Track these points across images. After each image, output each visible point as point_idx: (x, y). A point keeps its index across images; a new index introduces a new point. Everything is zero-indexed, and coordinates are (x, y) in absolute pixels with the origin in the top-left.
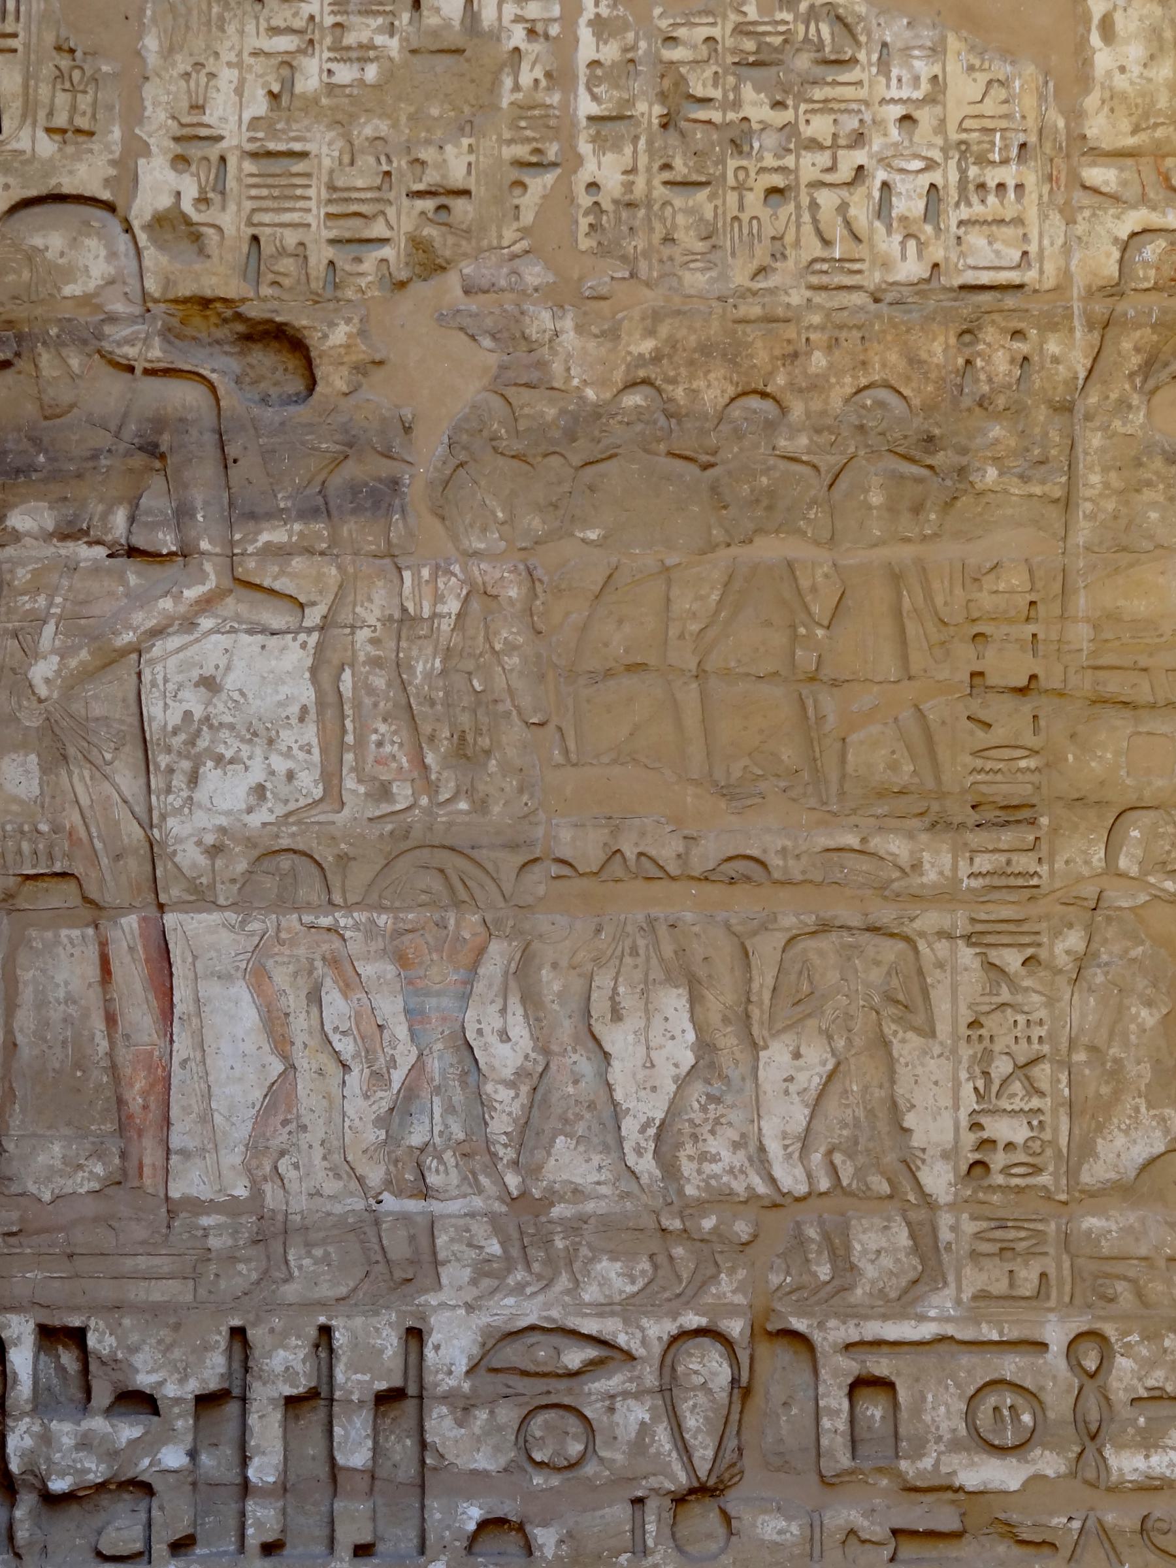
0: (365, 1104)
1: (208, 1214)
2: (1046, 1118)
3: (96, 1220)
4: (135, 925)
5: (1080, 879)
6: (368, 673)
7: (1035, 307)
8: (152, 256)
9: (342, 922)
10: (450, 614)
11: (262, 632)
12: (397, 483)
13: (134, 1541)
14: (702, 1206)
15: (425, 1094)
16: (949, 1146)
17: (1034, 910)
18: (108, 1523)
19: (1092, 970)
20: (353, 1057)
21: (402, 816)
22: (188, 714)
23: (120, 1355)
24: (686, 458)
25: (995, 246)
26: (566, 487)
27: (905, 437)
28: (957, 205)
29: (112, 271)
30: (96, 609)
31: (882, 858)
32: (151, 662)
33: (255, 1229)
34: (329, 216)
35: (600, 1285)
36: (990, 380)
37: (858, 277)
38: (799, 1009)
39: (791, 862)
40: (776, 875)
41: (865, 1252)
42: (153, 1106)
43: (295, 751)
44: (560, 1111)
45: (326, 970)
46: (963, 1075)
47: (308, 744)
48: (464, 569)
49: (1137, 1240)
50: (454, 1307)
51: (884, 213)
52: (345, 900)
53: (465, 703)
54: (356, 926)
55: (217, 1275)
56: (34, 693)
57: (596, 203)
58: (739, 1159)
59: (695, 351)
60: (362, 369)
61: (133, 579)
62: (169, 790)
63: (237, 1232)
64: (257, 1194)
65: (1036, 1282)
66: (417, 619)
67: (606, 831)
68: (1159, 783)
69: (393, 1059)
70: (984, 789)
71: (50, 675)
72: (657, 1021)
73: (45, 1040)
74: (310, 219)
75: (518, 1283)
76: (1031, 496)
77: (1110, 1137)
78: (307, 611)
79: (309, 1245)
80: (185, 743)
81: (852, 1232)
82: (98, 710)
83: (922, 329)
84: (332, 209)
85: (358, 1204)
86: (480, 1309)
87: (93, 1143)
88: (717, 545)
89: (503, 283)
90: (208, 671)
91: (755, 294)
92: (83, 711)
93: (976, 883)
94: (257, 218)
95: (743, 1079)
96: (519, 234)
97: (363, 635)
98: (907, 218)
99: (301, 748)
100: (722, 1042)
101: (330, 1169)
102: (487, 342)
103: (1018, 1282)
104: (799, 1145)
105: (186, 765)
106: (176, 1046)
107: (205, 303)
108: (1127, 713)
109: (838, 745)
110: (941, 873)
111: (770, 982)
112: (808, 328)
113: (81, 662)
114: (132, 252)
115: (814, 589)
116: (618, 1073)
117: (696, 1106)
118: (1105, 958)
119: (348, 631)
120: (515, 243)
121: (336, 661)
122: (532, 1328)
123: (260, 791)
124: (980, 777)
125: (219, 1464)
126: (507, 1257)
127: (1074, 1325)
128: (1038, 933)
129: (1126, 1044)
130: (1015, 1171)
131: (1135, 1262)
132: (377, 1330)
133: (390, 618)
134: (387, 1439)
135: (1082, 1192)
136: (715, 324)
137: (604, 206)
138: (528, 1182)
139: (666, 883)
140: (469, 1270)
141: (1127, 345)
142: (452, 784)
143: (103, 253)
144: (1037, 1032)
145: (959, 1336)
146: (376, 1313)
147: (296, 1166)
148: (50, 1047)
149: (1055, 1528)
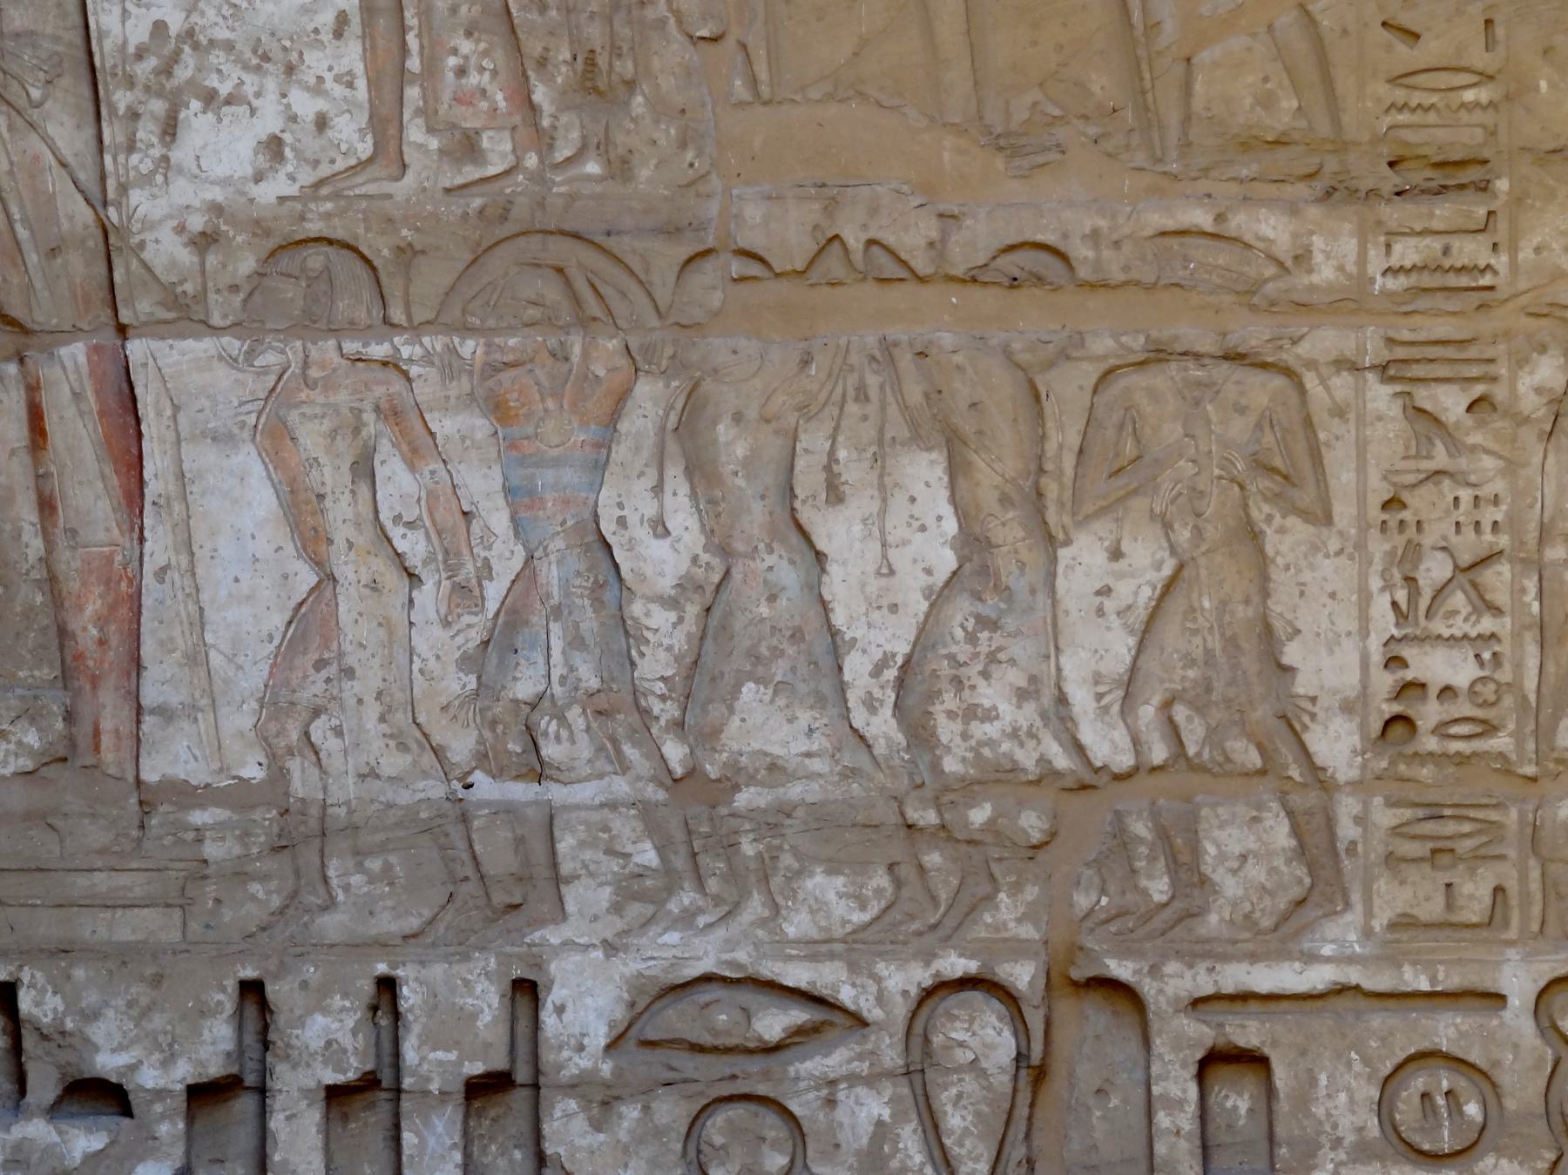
2: (1504, 648)
3: (29, 816)
4: (82, 359)
9: (406, 352)
14: (970, 789)
15: (537, 620)
16: (1352, 694)
17: (1487, 325)
20: (425, 563)
21: (497, 186)
22: (159, 27)
23: (69, 1025)
31: (1248, 246)
33: (276, 830)
35: (812, 912)
38: (1119, 482)
39: (1107, 253)
40: (1083, 273)
41: (1222, 857)
42: (114, 640)
43: (329, 84)
44: (747, 643)
45: (380, 426)
46: (1375, 583)
47: (349, 73)
50: (586, 947)
54: (427, 359)
55: (218, 901)
58: (1027, 715)
62: (131, 147)
63: (247, 834)
64: (278, 775)
65: (1488, 900)
67: (816, 206)
70: (1409, 136)
72: (898, 502)
75: (685, 910)
79: (359, 854)
80: (157, 72)
81: (1203, 826)
86: (626, 948)
87: (22, 698)
93: (1395, 284)
95: (1033, 592)
99: (337, 79)
100: (998, 534)
101: (391, 736)
103: (1461, 902)
104: (1120, 693)
105: (158, 106)
106: (148, 546)
109: (1180, 68)
111: (1074, 440)
116: (839, 585)
117: (959, 633)
122: (707, 979)
123: (274, 147)
124: (1402, 118)
126: (667, 870)
127: (1545, 967)
128: (1491, 361)
130: (1454, 730)
132: (466, 983)
134: (484, 1149)
135: (1559, 761)
138: (699, 753)
139: (911, 287)
140: (608, 890)
142: (575, 135)
144: (1490, 515)
145: (1368, 985)
146: (466, 958)
147: (338, 732)
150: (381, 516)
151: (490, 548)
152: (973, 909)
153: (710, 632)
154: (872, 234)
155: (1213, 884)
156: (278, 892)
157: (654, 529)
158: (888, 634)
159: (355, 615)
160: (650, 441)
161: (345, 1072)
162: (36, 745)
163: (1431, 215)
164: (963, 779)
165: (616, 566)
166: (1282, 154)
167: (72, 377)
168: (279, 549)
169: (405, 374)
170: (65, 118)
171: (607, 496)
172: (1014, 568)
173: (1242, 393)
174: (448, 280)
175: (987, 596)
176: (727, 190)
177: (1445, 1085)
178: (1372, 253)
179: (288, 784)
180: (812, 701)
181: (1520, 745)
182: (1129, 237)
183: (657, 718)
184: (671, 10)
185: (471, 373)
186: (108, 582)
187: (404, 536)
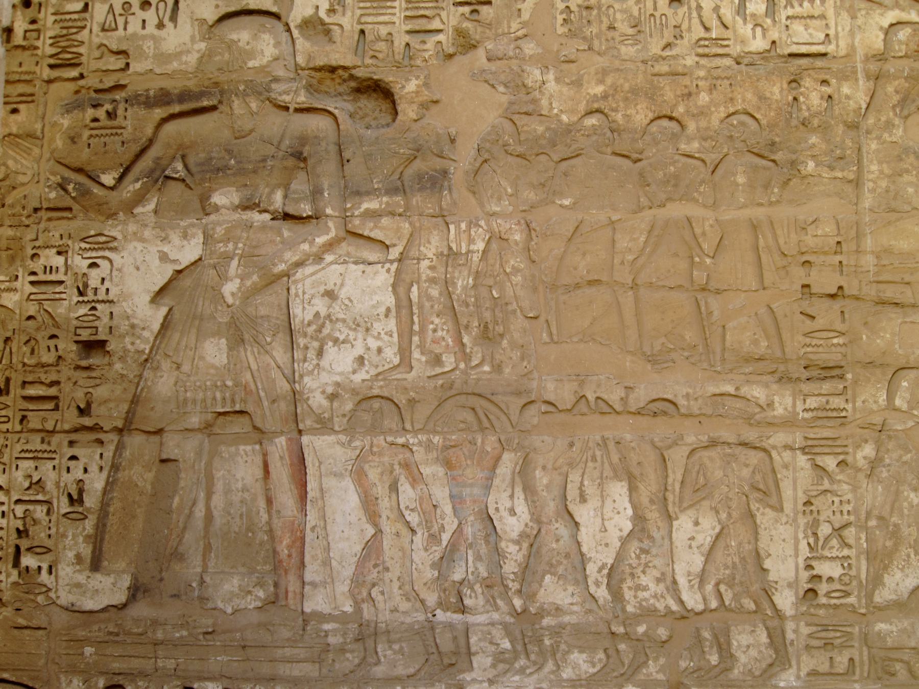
1: (328, 622)
2: (853, 562)
3: (260, 625)
4: (284, 443)
5: (872, 412)
6: (428, 287)
7: (835, 66)
8: (301, 43)
9: (411, 441)
10: (478, 251)
11: (363, 263)
12: (446, 173)
14: (638, 618)
15: (463, 549)
16: (792, 580)
17: (843, 432)
20: (418, 525)
21: (448, 375)
24: (624, 156)
25: (809, 31)
26: (550, 174)
27: (758, 143)
28: (786, 7)
29: (277, 52)
30: (262, 251)
31: (748, 400)
32: (296, 282)
33: (357, 632)
34: (406, 17)
35: (573, 668)
36: (809, 109)
37: (727, 49)
38: (699, 494)
40: (683, 410)
41: (739, 646)
42: (294, 555)
43: (383, 335)
44: (547, 559)
45: (401, 470)
46: (801, 535)
48: (487, 224)
49: (909, 637)
50: (481, 682)
51: (741, 11)
52: (413, 427)
53: (487, 305)
54: (420, 443)
55: (333, 661)
56: (225, 302)
57: (567, 7)
58: (661, 588)
59: (628, 92)
60: (425, 106)
61: (286, 234)
62: (305, 360)
65: (847, 664)
66: (458, 254)
69: (443, 526)
70: (811, 356)
71: (235, 290)
72: (609, 504)
73: (229, 514)
74: (395, 19)
75: (521, 667)
76: (835, 178)
77: (892, 573)
78: (390, 250)
79: (389, 641)
80: (316, 331)
81: (731, 634)
82: (263, 311)
83: (766, 79)
84: (408, 13)
85: (421, 617)
86: (497, 682)
87: (258, 578)
88: (643, 208)
89: (511, 54)
90: (330, 287)
91: (664, 59)
93: (807, 415)
94: (363, 20)
96: (521, 26)
97: (425, 264)
98: (755, 15)
99: (386, 334)
100: (649, 515)
102: (501, 89)
103: (836, 664)
104: (698, 580)
105: (316, 344)
106: (308, 518)
107: (333, 70)
108: (898, 310)
109: (720, 329)
110: (786, 409)
111: (679, 477)
112: (697, 79)
113: (253, 283)
114: (290, 42)
115: (704, 234)
116: (584, 535)
117: (633, 555)
118: (887, 461)
119: (415, 261)
120: (518, 30)
121: (408, 280)
123: (361, 360)
124: (809, 349)
126: (514, 650)
129: (902, 515)
130: (833, 595)
133: (442, 254)
135: (874, 607)
136: (640, 77)
137: (572, 9)
138: (528, 603)
139: (613, 416)
141: (890, 89)
142: (480, 355)
143: (272, 42)
144: (846, 508)
147: (382, 593)
148: (233, 518)
151: (444, 519)
152: (638, 667)
153: (532, 554)
155: (736, 657)
163: (821, 388)
164: (634, 614)
165: (495, 528)
166: (761, 364)
169: (411, 450)
170: (280, 349)
174: (429, 412)
176: (540, 378)
178: (798, 403)
179: (362, 614)
181: (859, 601)
186: (292, 531)
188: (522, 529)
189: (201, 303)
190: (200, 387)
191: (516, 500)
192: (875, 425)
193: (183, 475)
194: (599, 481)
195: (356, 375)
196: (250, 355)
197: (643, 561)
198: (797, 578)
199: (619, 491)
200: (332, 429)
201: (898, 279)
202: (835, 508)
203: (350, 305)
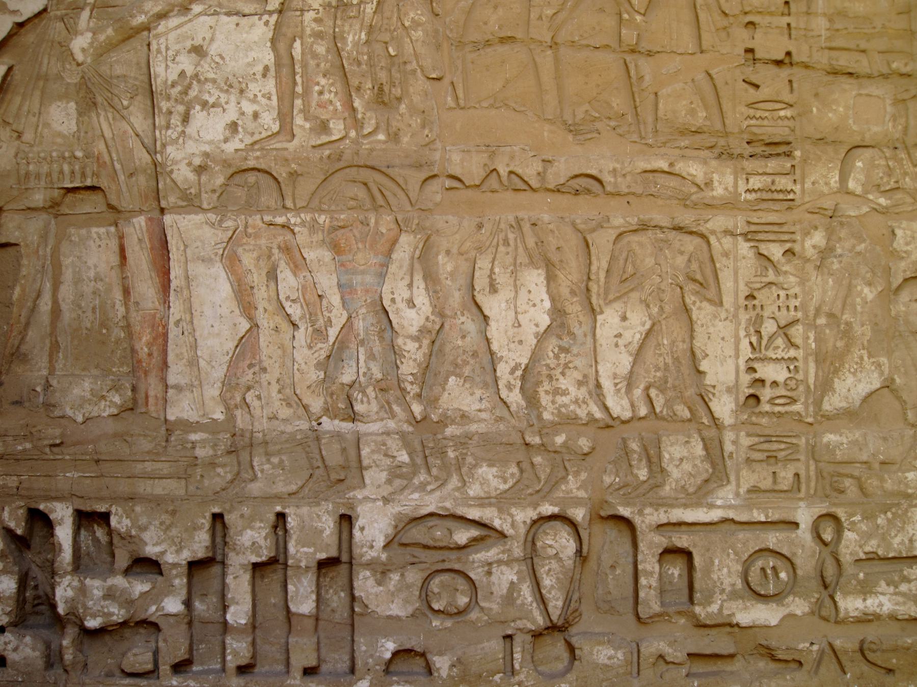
0: (309, 353)
1: (195, 432)
2: (800, 364)
3: (116, 435)
4: (143, 224)
5: (822, 195)
6: (313, 43)
9: (293, 221)
13: (147, 663)
15: (353, 346)
16: (731, 384)
18: (129, 649)
19: (830, 260)
20: (300, 319)
21: (337, 145)
22: (182, 74)
23: (133, 533)
31: (684, 178)
32: (157, 36)
33: (229, 443)
35: (481, 484)
38: (627, 284)
39: (619, 180)
40: (609, 188)
41: (672, 459)
42: (155, 354)
43: (259, 98)
44: (451, 358)
45: (281, 255)
46: (742, 333)
47: (269, 93)
49: (861, 449)
50: (375, 500)
52: (295, 205)
53: (383, 64)
54: (303, 224)
55: (202, 476)
56: (74, 59)
58: (582, 393)
62: (168, 127)
63: (216, 445)
64: (231, 417)
65: (791, 479)
68: (875, 129)
69: (330, 320)
70: (755, 130)
71: (85, 46)
72: (523, 295)
73: (80, 307)
75: (421, 483)
77: (843, 377)
79: (268, 454)
80: (181, 93)
81: (663, 445)
82: (119, 70)
85: (304, 425)
86: (393, 500)
90: (198, 42)
92: (108, 72)
93: (751, 197)
95: (585, 335)
97: (309, 16)
99: (263, 96)
100: (570, 309)
101: (284, 400)
103: (779, 480)
104: (625, 383)
105: (181, 108)
106: (172, 310)
109: (652, 97)
110: (726, 189)
111: (605, 265)
113: (108, 37)
116: (494, 331)
117: (551, 354)
118: (839, 251)
119: (298, 13)
121: (290, 35)
122: (431, 515)
123: (233, 127)
124: (753, 122)
125: (208, 609)
126: (413, 463)
127: (817, 510)
128: (793, 233)
129: (854, 312)
130: (777, 401)
131: (858, 465)
132: (318, 516)
134: (327, 591)
135: (822, 416)
138: (428, 410)
139: (529, 194)
140: (385, 473)
142: (373, 122)
144: (793, 303)
145: (737, 518)
146: (318, 504)
147: (259, 398)
148: (84, 312)
149: (801, 651)
150: (280, 297)
151: (331, 312)
152: (557, 483)
153: (434, 353)
154: (511, 169)
156: (230, 472)
157: (408, 304)
158: (518, 354)
159: (267, 343)
160: (407, 263)
161: (261, 557)
162: (119, 402)
163: (766, 166)
164: (552, 422)
165: (390, 321)
166: (698, 137)
167: (138, 232)
168: (232, 311)
169: (292, 231)
170: (139, 114)
171: (386, 289)
172: (576, 324)
173: (682, 245)
174: (314, 187)
175: (564, 337)
177: (771, 564)
178: (740, 182)
180: (482, 385)
181: (807, 408)
182: (629, 172)
183: (409, 393)
184: (419, 65)
185: (323, 231)
186: (153, 326)
187: (291, 306)
188: (422, 323)
189: (45, 61)
190: (45, 159)
191: (415, 289)
192: (826, 209)
193: (25, 262)
194: (512, 268)
195: (228, 144)
196: (103, 122)
197: (562, 361)
198: (737, 381)
199: (535, 279)
200: (200, 207)
201: (852, 45)
202: (780, 303)
203: (221, 62)
